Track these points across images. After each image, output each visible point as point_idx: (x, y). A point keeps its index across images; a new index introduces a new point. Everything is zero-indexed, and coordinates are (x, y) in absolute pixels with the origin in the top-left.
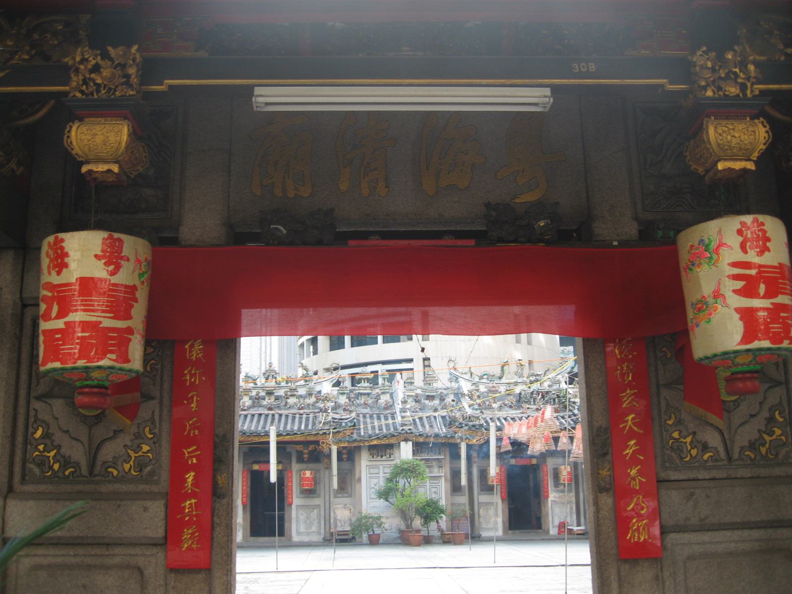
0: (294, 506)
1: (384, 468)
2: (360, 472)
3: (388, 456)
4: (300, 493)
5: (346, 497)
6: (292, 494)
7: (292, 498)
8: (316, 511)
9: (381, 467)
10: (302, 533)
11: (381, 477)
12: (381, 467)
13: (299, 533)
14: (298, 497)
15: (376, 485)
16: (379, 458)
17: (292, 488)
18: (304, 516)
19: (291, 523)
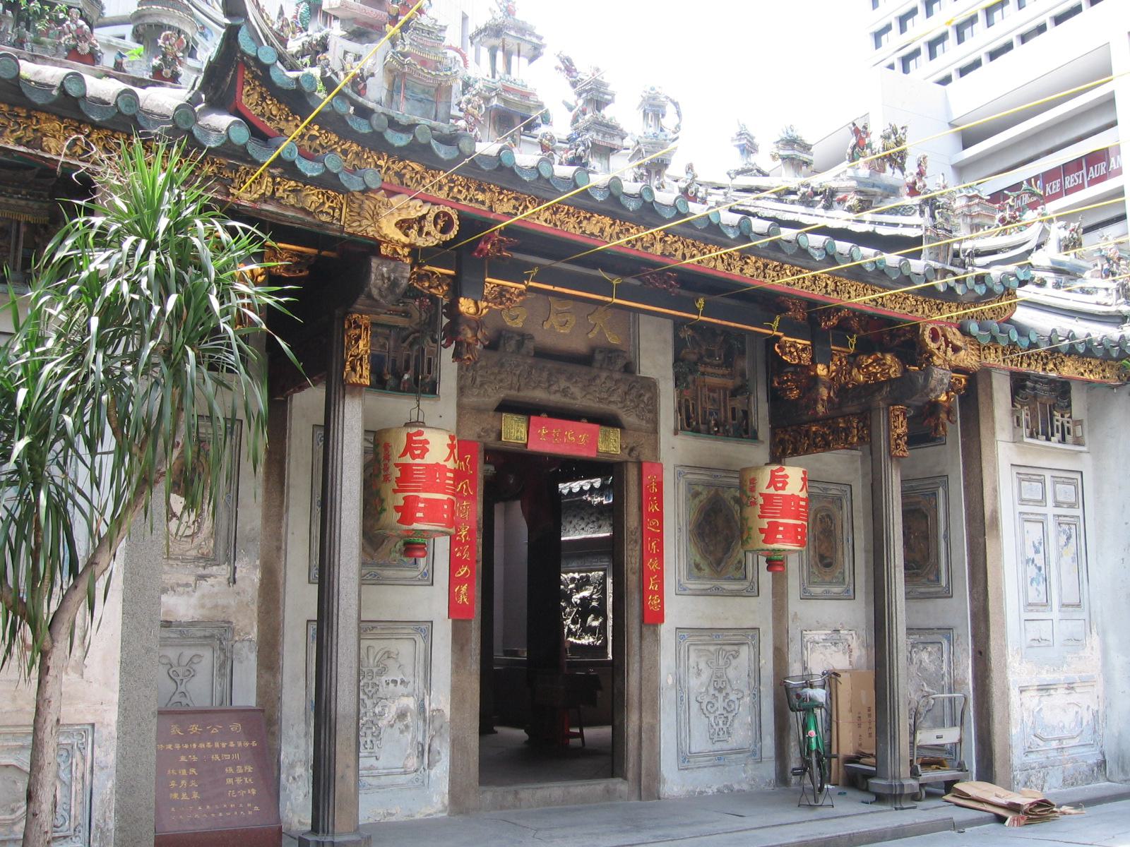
0: (666, 631)
1: (1056, 481)
2: (995, 490)
3: (1058, 436)
4: (690, 575)
5: (837, 598)
6: (660, 574)
7: (660, 593)
8: (745, 652)
9: (1048, 475)
10: (698, 754)
11: (1050, 518)
12: (1048, 475)
13: (686, 759)
14: (681, 591)
15: (1037, 552)
16: (1041, 442)
17: (660, 546)
18: (705, 676)
19: (655, 712)
